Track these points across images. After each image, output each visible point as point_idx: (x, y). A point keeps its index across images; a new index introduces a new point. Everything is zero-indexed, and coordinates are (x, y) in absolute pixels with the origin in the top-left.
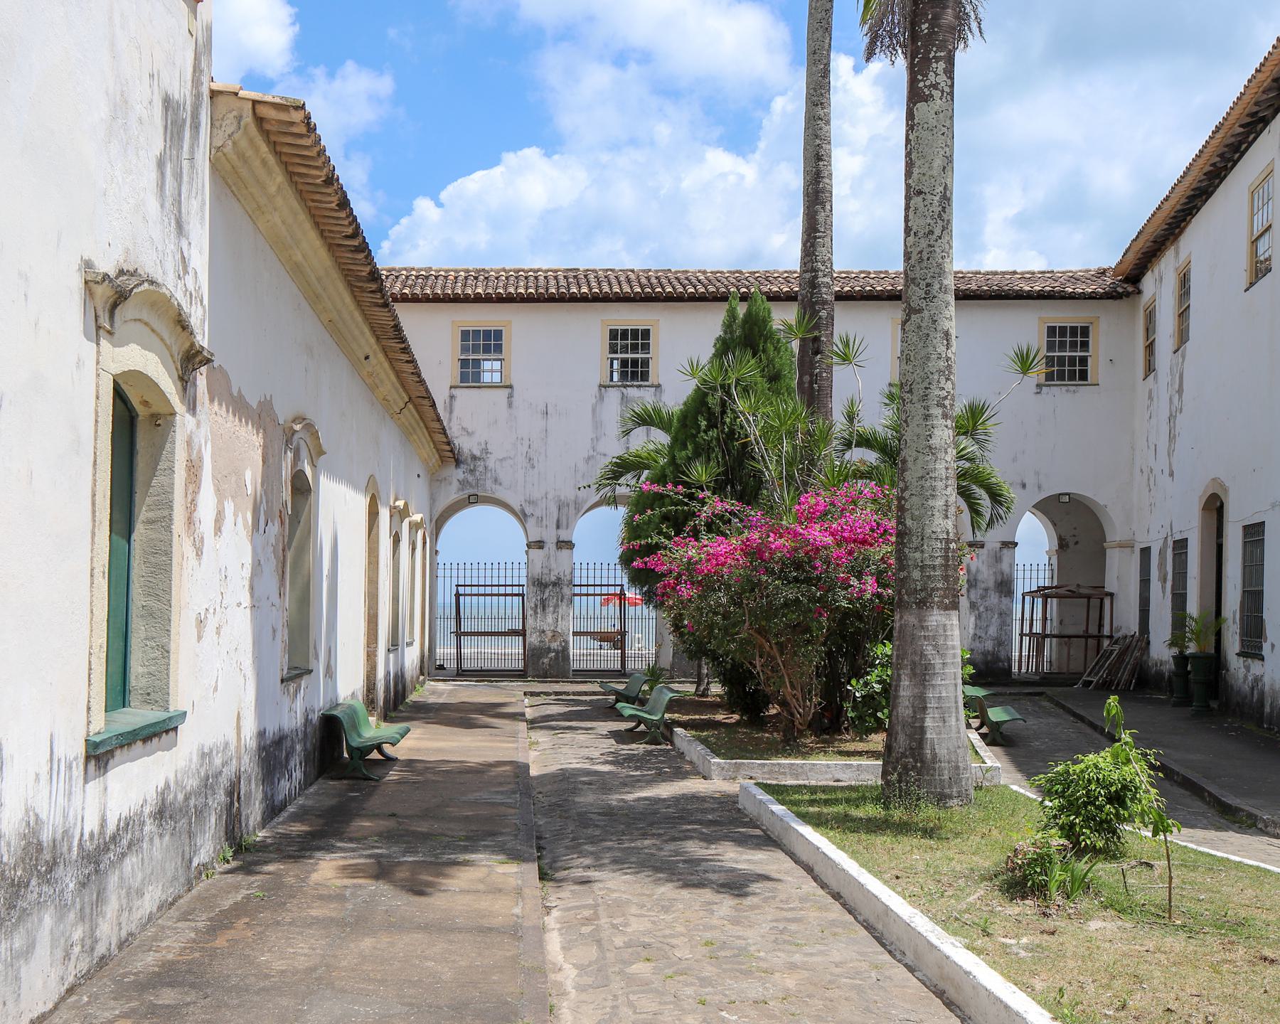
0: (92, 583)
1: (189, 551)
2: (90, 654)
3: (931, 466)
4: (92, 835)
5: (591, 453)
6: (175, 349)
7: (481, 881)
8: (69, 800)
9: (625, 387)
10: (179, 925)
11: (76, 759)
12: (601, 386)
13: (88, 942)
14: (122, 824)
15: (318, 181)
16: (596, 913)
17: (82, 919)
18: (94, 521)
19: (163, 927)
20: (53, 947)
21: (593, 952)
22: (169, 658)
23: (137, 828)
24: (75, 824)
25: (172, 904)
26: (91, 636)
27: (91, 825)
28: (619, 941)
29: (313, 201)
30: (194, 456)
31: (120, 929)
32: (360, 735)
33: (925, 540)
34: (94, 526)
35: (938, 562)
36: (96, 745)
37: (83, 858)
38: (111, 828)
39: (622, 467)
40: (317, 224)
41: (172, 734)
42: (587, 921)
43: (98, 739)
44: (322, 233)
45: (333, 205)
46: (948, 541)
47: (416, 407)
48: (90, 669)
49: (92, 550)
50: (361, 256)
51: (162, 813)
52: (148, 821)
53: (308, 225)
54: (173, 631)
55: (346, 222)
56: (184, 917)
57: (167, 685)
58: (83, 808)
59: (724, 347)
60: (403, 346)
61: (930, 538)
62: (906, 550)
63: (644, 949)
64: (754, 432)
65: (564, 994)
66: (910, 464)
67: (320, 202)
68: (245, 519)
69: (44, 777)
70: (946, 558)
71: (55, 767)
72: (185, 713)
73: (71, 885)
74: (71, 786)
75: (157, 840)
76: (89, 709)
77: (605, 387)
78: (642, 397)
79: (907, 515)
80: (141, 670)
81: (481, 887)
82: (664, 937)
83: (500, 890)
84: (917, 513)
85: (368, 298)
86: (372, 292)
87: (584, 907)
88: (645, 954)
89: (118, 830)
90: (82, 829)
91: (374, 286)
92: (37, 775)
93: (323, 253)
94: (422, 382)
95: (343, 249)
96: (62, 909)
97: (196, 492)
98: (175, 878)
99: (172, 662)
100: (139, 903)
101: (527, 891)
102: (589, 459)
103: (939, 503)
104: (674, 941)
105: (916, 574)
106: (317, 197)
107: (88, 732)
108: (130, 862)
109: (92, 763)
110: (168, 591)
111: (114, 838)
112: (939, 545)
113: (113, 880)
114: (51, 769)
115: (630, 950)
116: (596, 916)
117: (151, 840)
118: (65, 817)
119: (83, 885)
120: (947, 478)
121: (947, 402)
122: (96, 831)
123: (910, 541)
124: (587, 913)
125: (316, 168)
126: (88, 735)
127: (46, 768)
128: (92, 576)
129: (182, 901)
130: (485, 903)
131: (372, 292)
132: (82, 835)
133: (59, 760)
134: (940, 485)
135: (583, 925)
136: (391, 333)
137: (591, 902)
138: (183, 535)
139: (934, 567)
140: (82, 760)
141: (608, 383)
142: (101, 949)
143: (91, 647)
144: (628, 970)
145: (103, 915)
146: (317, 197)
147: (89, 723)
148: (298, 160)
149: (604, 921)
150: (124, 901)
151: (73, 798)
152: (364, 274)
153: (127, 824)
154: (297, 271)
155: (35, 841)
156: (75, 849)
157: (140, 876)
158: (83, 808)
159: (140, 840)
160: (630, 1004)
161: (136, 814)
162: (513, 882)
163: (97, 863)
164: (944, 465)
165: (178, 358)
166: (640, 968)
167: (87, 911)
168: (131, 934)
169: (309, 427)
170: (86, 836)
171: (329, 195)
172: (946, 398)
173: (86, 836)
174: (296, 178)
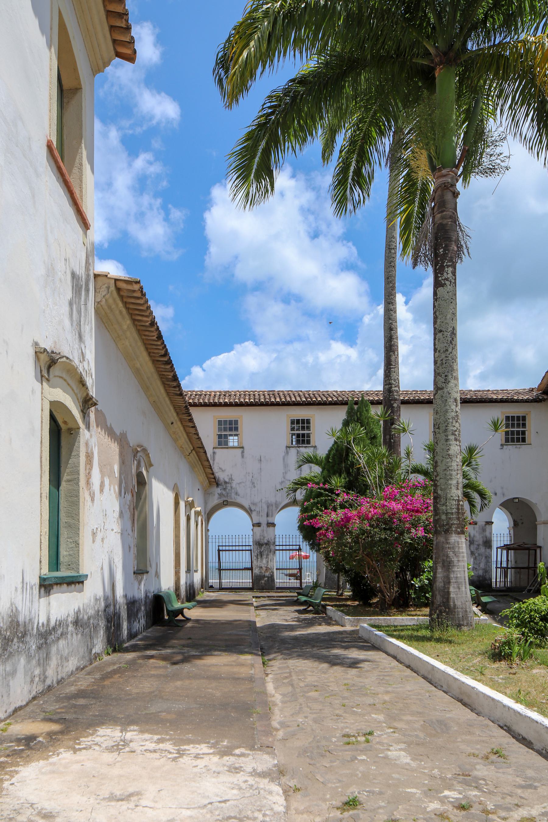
0: (41, 500)
1: (88, 498)
2: (41, 535)
3: (450, 464)
4: (43, 624)
6: (79, 396)
7: (233, 661)
8: (32, 604)
10: (86, 677)
11: (35, 585)
13: (42, 677)
14: (58, 623)
15: (147, 324)
18: (41, 470)
19: (79, 678)
21: (290, 689)
22: (79, 547)
23: (65, 627)
24: (35, 617)
25: (83, 669)
26: (41, 527)
27: (43, 619)
29: (145, 335)
30: (89, 451)
31: (58, 675)
32: (172, 606)
33: (448, 500)
34: (41, 473)
35: (454, 511)
36: (44, 579)
37: (39, 635)
38: (52, 623)
40: (147, 349)
41: (81, 585)
42: (286, 678)
43: (45, 577)
44: (149, 354)
45: (155, 338)
46: (459, 501)
47: (196, 452)
48: (41, 542)
49: (41, 484)
50: (168, 367)
51: (77, 622)
52: (71, 625)
53: (142, 349)
54: (81, 535)
55: (161, 347)
56: (89, 674)
57: (78, 560)
59: (346, 423)
60: (190, 418)
61: (450, 499)
62: (438, 506)
63: (315, 687)
64: (363, 462)
65: (275, 705)
66: (439, 464)
68: (114, 488)
69: (20, 590)
70: (458, 509)
71: (25, 586)
72: (87, 575)
74: (33, 598)
75: (74, 635)
76: (40, 562)
79: (439, 488)
80: (65, 553)
81: (234, 663)
82: (324, 683)
83: (243, 665)
84: (443, 487)
86: (174, 387)
87: (285, 673)
88: (315, 689)
89: (56, 625)
90: (38, 620)
92: (16, 588)
93: (150, 364)
94: (199, 439)
95: (160, 363)
98: (83, 657)
99: (80, 549)
100: (67, 664)
101: (256, 665)
103: (454, 482)
105: (444, 517)
106: (147, 333)
108: (62, 643)
110: (78, 514)
111: (54, 628)
112: (454, 503)
113: (54, 649)
114: (23, 586)
115: (307, 688)
116: (291, 676)
117: (72, 634)
118: (30, 612)
122: (45, 623)
123: (440, 501)
124: (286, 675)
126: (40, 575)
128: (41, 497)
129: (87, 668)
130: (236, 669)
131: (174, 387)
132: (38, 623)
133: (27, 583)
134: (454, 473)
135: (284, 679)
137: (288, 671)
138: (85, 488)
139: (452, 514)
140: (38, 587)
142: (48, 682)
143: (41, 532)
144: (307, 695)
145: (48, 664)
146: (147, 333)
147: (41, 569)
148: (137, 312)
149: (294, 677)
150: (59, 661)
152: (170, 377)
153: (60, 623)
156: (35, 629)
157: (66, 651)
158: (39, 610)
159: (67, 633)
160: (308, 707)
161: (64, 620)
162: (249, 662)
163: (46, 639)
165: (81, 400)
166: (313, 694)
167: (42, 661)
168: (62, 678)
169: (145, 450)
170: (40, 624)
171: (152, 332)
173: (40, 624)
174: (136, 323)
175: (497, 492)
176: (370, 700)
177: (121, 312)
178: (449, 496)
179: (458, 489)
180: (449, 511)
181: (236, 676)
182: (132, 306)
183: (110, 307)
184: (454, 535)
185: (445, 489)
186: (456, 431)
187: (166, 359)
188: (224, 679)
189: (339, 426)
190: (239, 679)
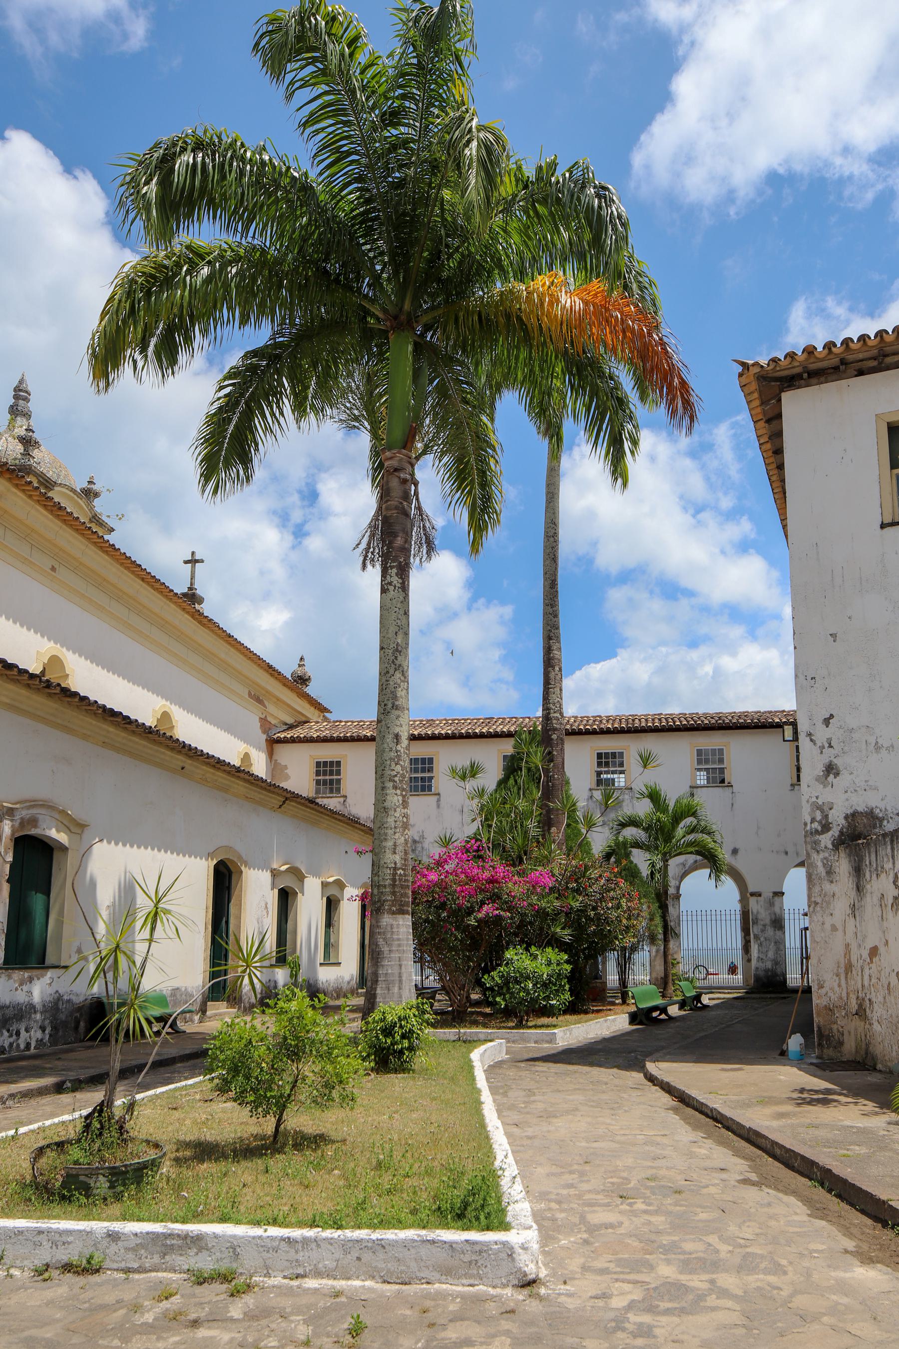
103: (389, 844)
120: (395, 827)
121: (396, 779)
164: (393, 819)
172: (396, 776)
175: (788, 850)
179: (395, 853)
186: (396, 776)
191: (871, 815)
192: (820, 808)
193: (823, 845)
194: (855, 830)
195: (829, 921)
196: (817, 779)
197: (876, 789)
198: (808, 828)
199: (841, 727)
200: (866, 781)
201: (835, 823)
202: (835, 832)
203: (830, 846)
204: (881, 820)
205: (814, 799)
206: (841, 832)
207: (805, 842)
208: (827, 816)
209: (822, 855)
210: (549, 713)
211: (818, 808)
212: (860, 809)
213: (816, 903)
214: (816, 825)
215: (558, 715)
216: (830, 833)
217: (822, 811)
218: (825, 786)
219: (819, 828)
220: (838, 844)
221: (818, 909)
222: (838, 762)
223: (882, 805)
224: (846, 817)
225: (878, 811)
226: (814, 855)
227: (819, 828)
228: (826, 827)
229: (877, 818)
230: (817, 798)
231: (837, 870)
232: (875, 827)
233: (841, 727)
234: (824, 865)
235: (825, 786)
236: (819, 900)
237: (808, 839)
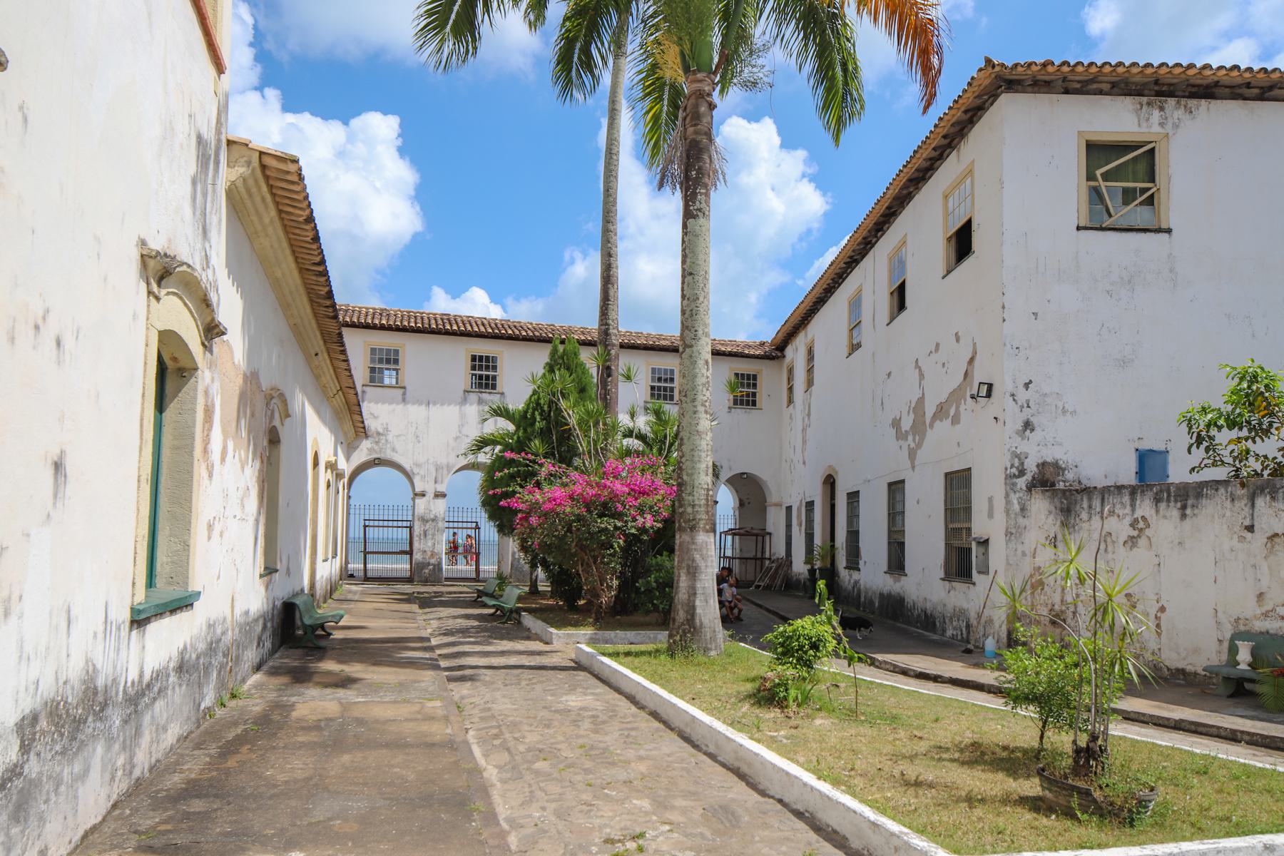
4: (133, 683)
5: (458, 434)
8: (118, 654)
9: (482, 392)
10: (195, 752)
11: (124, 622)
12: (465, 391)
14: (154, 675)
15: (301, 219)
16: (500, 731)
17: (124, 748)
19: (182, 755)
20: (103, 770)
21: (505, 757)
23: (164, 679)
24: (121, 674)
27: (133, 675)
28: (522, 748)
29: (294, 234)
31: (151, 757)
33: (695, 489)
35: (703, 502)
36: (139, 612)
37: (126, 701)
38: (147, 678)
39: (482, 443)
40: (293, 252)
43: (141, 607)
44: (296, 258)
45: (308, 239)
53: (288, 252)
55: (316, 253)
58: (127, 662)
59: (551, 368)
62: (684, 495)
63: (539, 752)
64: (573, 421)
67: (299, 235)
70: (707, 500)
73: (117, 722)
74: (119, 643)
76: (134, 584)
77: (468, 392)
78: (492, 399)
79: (684, 473)
85: (322, 310)
88: (542, 755)
89: (152, 680)
90: (126, 678)
91: (328, 303)
93: (296, 274)
95: (310, 273)
96: (110, 740)
97: (210, 429)
100: (164, 736)
102: (457, 438)
104: (559, 746)
105: (689, 510)
106: (297, 231)
107: (133, 602)
108: (159, 705)
109: (135, 626)
111: (149, 686)
113: (147, 718)
115: (531, 754)
118: (115, 667)
119: (125, 722)
122: (136, 680)
123: (686, 489)
125: (301, 209)
126: (133, 605)
127: (101, 628)
132: (126, 682)
133: (112, 623)
136: (335, 338)
139: (700, 506)
140: (127, 624)
141: (470, 389)
144: (533, 767)
145: (138, 745)
146: (297, 231)
147: (133, 595)
150: (154, 735)
151: (121, 653)
153: (159, 675)
154: (276, 285)
155: (92, 686)
156: (121, 693)
157: (165, 716)
158: (127, 662)
159: (166, 688)
161: (164, 668)
163: (136, 705)
166: (540, 765)
168: (158, 761)
170: (129, 684)
171: (307, 230)
173: (129, 684)
174: (284, 215)
176: (622, 775)
177: (263, 199)
178: (696, 484)
179: (707, 475)
180: (697, 502)
181: (429, 740)
182: (280, 192)
183: (248, 191)
184: (701, 533)
185: (692, 474)
187: (321, 269)
188: (412, 746)
189: (540, 371)
190: (433, 745)
191: (1056, 466)
192: (1018, 456)
193: (1019, 487)
194: (1043, 476)
195: (1020, 548)
196: (1017, 433)
197: (1061, 444)
198: (1008, 472)
199: (1037, 392)
200: (1054, 438)
201: (1029, 470)
202: (1028, 477)
203: (1025, 488)
204: (1064, 470)
205: (1014, 449)
206: (1034, 478)
207: (1006, 484)
208: (1022, 464)
209: (1018, 495)
210: (608, 329)
211: (1016, 457)
212: (1049, 460)
213: (1012, 534)
214: (1014, 471)
215: (615, 331)
216: (1025, 478)
217: (1020, 459)
218: (1023, 439)
219: (1017, 473)
220: (1031, 487)
221: (1013, 538)
222: (1034, 420)
223: (1064, 458)
224: (1038, 466)
225: (1061, 463)
226: (1012, 495)
227: (1017, 473)
228: (1022, 473)
229: (1061, 468)
230: (1016, 448)
231: (1029, 508)
232: (1059, 475)
233: (1037, 392)
234: (1019, 503)
235: (1023, 439)
236: (1014, 531)
237: (1008, 481)
